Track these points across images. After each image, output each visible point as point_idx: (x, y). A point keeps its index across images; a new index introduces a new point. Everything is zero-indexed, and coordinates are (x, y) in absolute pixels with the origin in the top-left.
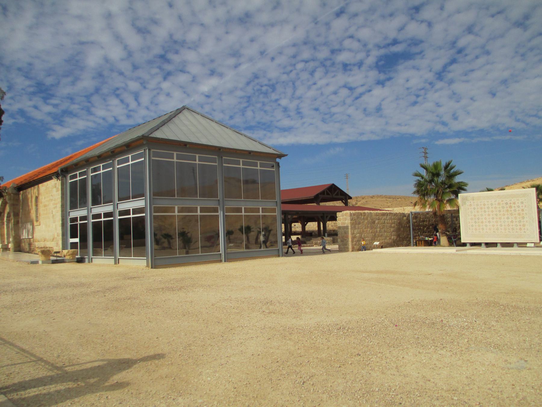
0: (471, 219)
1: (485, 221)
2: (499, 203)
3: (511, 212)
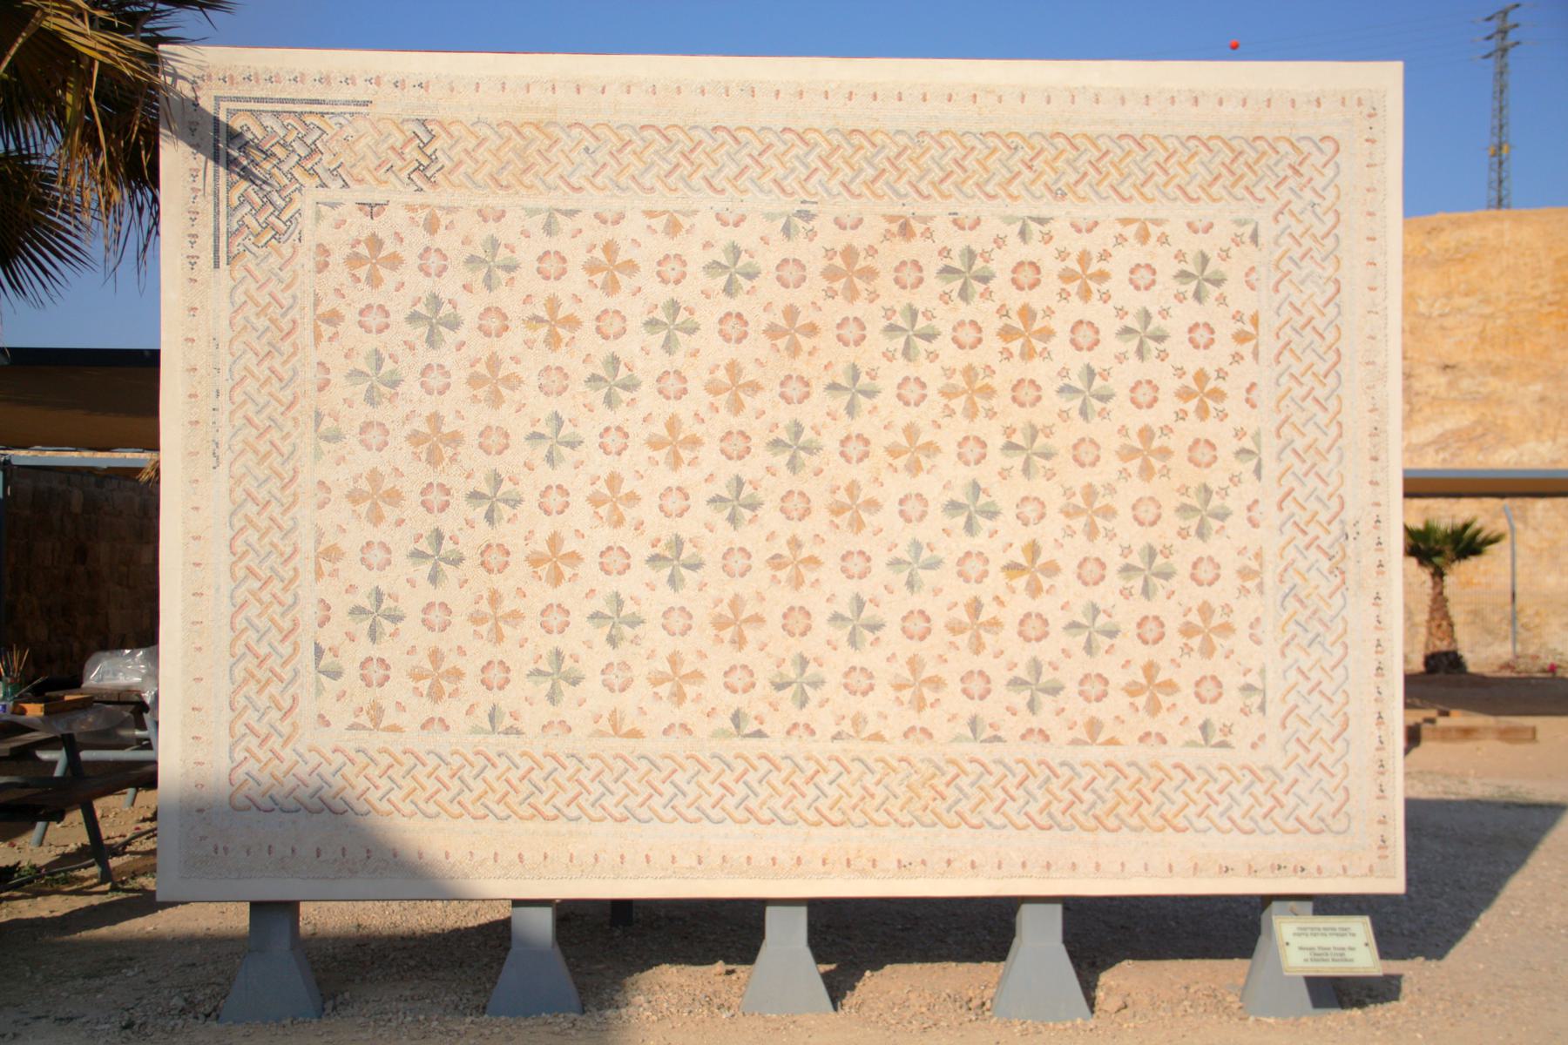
0: (354, 497)
1: (604, 536)
2: (850, 253)
3: (1018, 417)
